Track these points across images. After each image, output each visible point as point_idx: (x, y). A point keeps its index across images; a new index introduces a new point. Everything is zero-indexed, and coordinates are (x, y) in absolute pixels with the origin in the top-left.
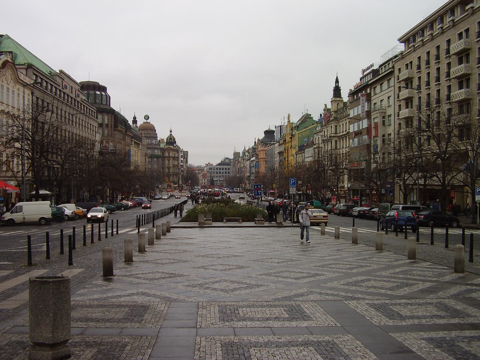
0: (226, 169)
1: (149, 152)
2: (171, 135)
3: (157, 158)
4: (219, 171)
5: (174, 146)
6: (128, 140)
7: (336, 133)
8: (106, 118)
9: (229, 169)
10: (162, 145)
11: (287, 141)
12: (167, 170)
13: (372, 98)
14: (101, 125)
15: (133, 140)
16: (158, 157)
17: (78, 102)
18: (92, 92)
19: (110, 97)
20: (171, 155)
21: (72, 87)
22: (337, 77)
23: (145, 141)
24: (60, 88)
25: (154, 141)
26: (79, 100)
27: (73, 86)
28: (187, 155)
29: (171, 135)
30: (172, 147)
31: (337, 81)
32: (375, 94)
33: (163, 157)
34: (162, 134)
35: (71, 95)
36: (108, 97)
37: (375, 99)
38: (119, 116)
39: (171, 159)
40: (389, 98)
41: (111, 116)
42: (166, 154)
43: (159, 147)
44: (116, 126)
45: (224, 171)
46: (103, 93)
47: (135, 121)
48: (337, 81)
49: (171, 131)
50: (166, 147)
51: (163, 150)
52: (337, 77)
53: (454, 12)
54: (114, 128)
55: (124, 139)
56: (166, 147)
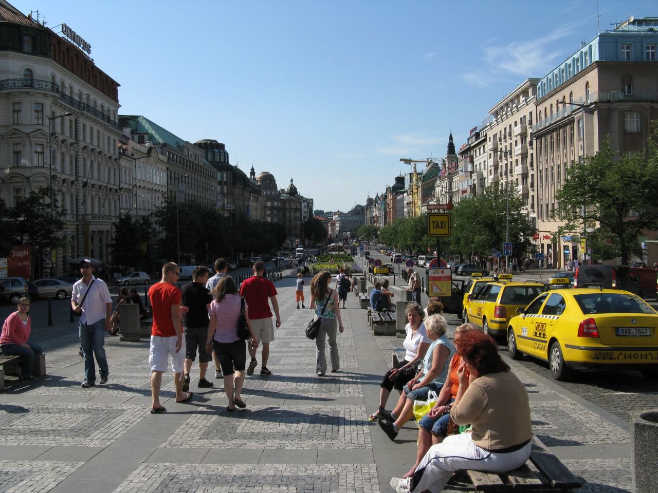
1: (269, 204)
2: (292, 184)
5: (295, 197)
6: (246, 194)
8: (225, 175)
11: (414, 191)
13: (474, 160)
14: (220, 183)
15: (252, 194)
17: (201, 167)
19: (228, 154)
21: (196, 155)
22: (451, 135)
23: (265, 193)
24: (187, 158)
25: (273, 193)
26: (202, 164)
27: (197, 153)
28: (312, 203)
29: (292, 184)
30: (293, 197)
31: (451, 138)
32: (476, 157)
34: (282, 184)
35: (195, 162)
36: (226, 154)
37: (477, 161)
38: (237, 172)
40: (484, 162)
41: (230, 173)
42: (288, 206)
44: (234, 183)
46: (222, 151)
47: (253, 173)
48: (451, 138)
49: (292, 181)
52: (451, 135)
53: (528, 93)
54: (233, 185)
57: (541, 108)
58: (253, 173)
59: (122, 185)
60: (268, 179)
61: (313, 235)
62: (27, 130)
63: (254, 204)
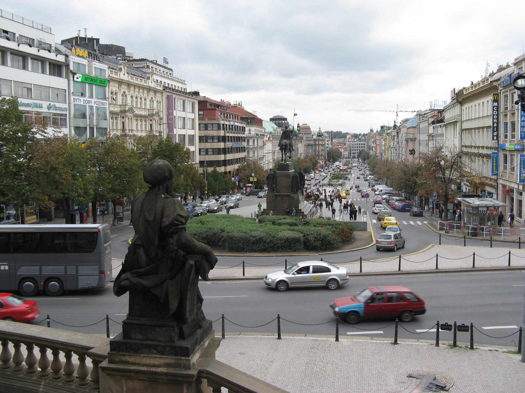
0: (362, 144)
2: (320, 130)
3: (311, 146)
4: (356, 146)
7: (394, 146)
9: (364, 144)
10: (315, 137)
12: (317, 153)
16: (312, 145)
18: (280, 122)
20: (320, 143)
25: (309, 136)
29: (320, 130)
30: (321, 138)
31: (395, 122)
33: (315, 145)
34: (314, 129)
39: (320, 146)
42: (317, 143)
43: (312, 139)
45: (361, 146)
46: (286, 122)
49: (320, 128)
50: (317, 138)
51: (315, 140)
55: (295, 142)
56: (317, 138)
57: (408, 130)
58: (298, 126)
59: (264, 154)
60: (307, 129)
61: (332, 159)
62: (251, 147)
63: (300, 145)
